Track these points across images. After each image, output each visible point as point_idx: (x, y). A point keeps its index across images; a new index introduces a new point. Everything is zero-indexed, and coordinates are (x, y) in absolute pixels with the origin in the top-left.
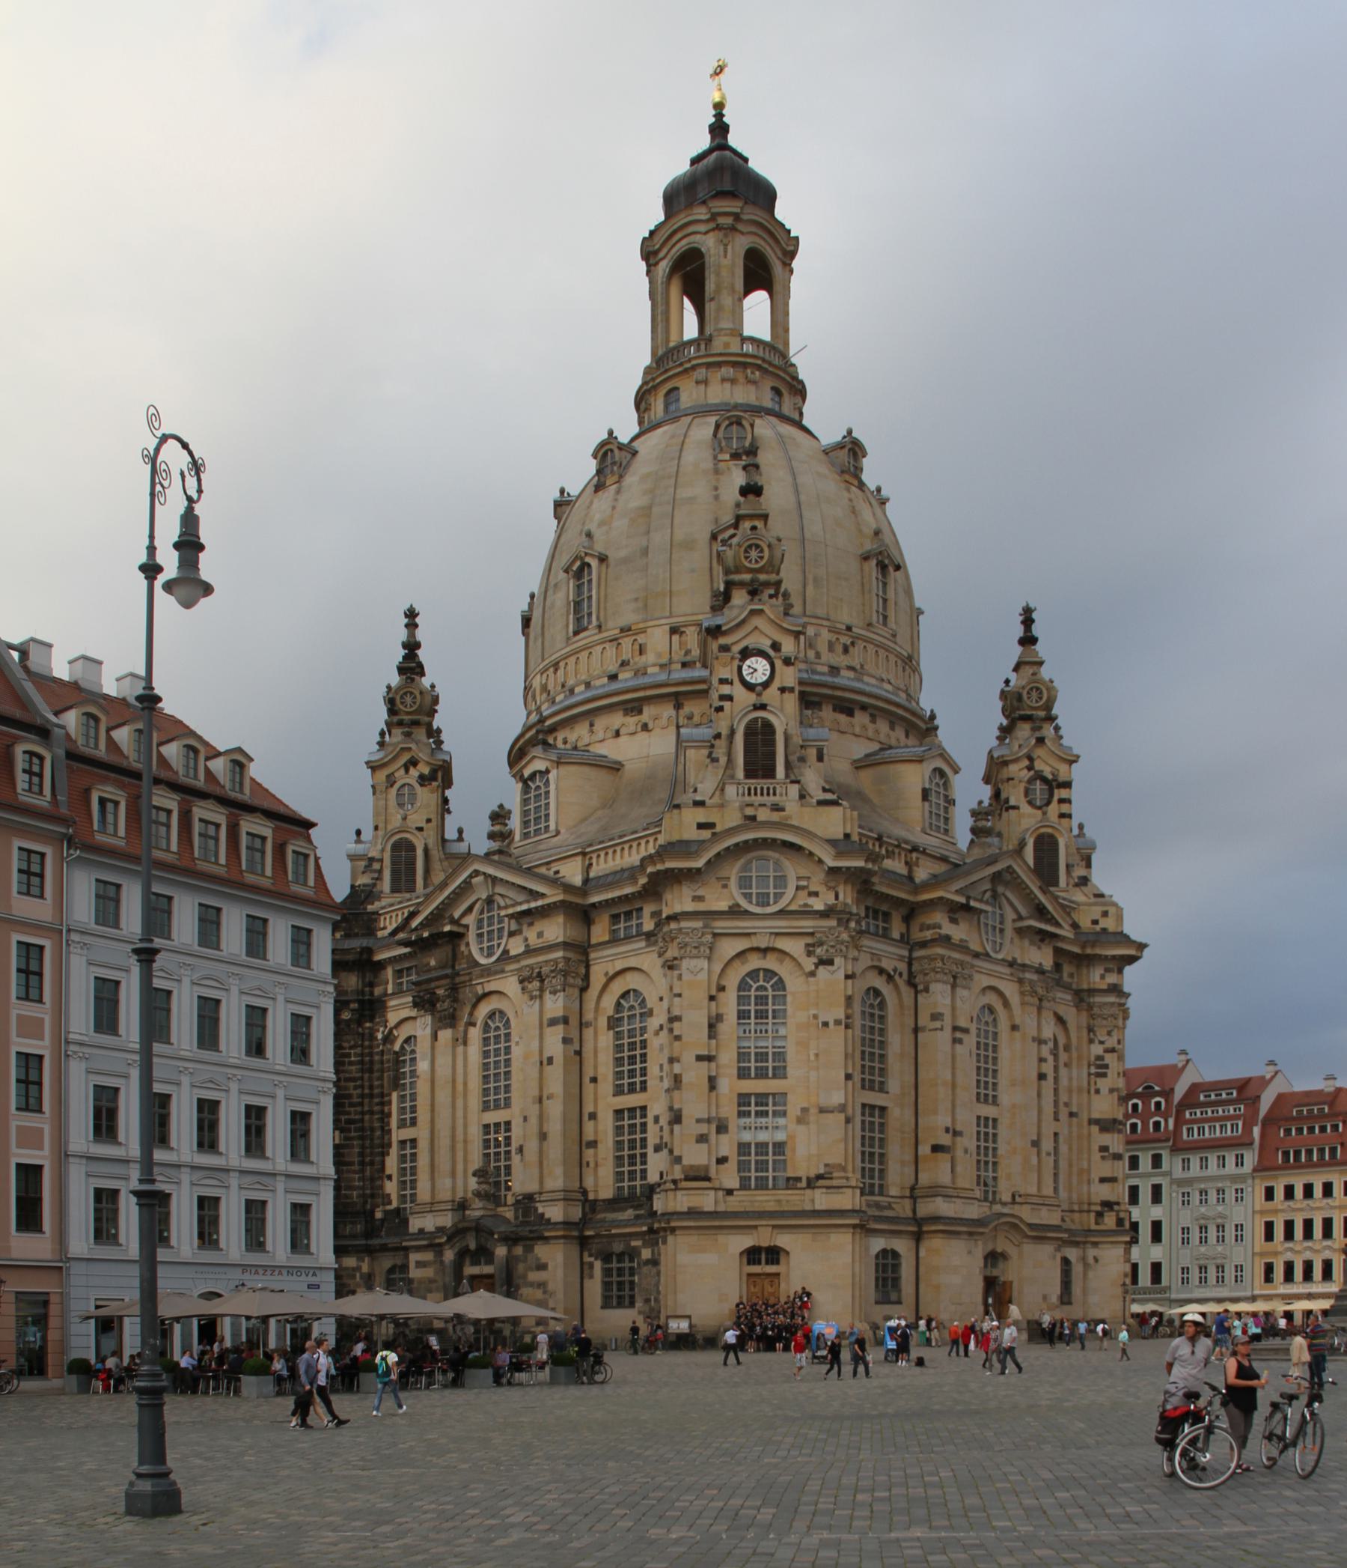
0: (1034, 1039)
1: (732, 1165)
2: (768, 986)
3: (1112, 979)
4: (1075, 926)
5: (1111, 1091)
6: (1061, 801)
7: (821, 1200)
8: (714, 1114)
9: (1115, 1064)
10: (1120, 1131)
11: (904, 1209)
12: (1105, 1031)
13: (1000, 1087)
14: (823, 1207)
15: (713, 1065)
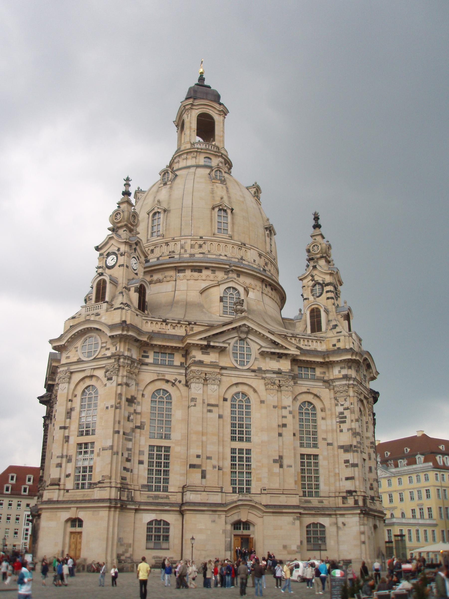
0: (275, 407)
1: (72, 478)
2: (93, 392)
3: (345, 372)
4: (298, 348)
5: (348, 430)
6: (327, 292)
7: (97, 494)
8: (65, 454)
9: (349, 415)
10: (354, 451)
11: (177, 499)
12: (343, 399)
13: (252, 433)
14: (97, 498)
15: (67, 431)
